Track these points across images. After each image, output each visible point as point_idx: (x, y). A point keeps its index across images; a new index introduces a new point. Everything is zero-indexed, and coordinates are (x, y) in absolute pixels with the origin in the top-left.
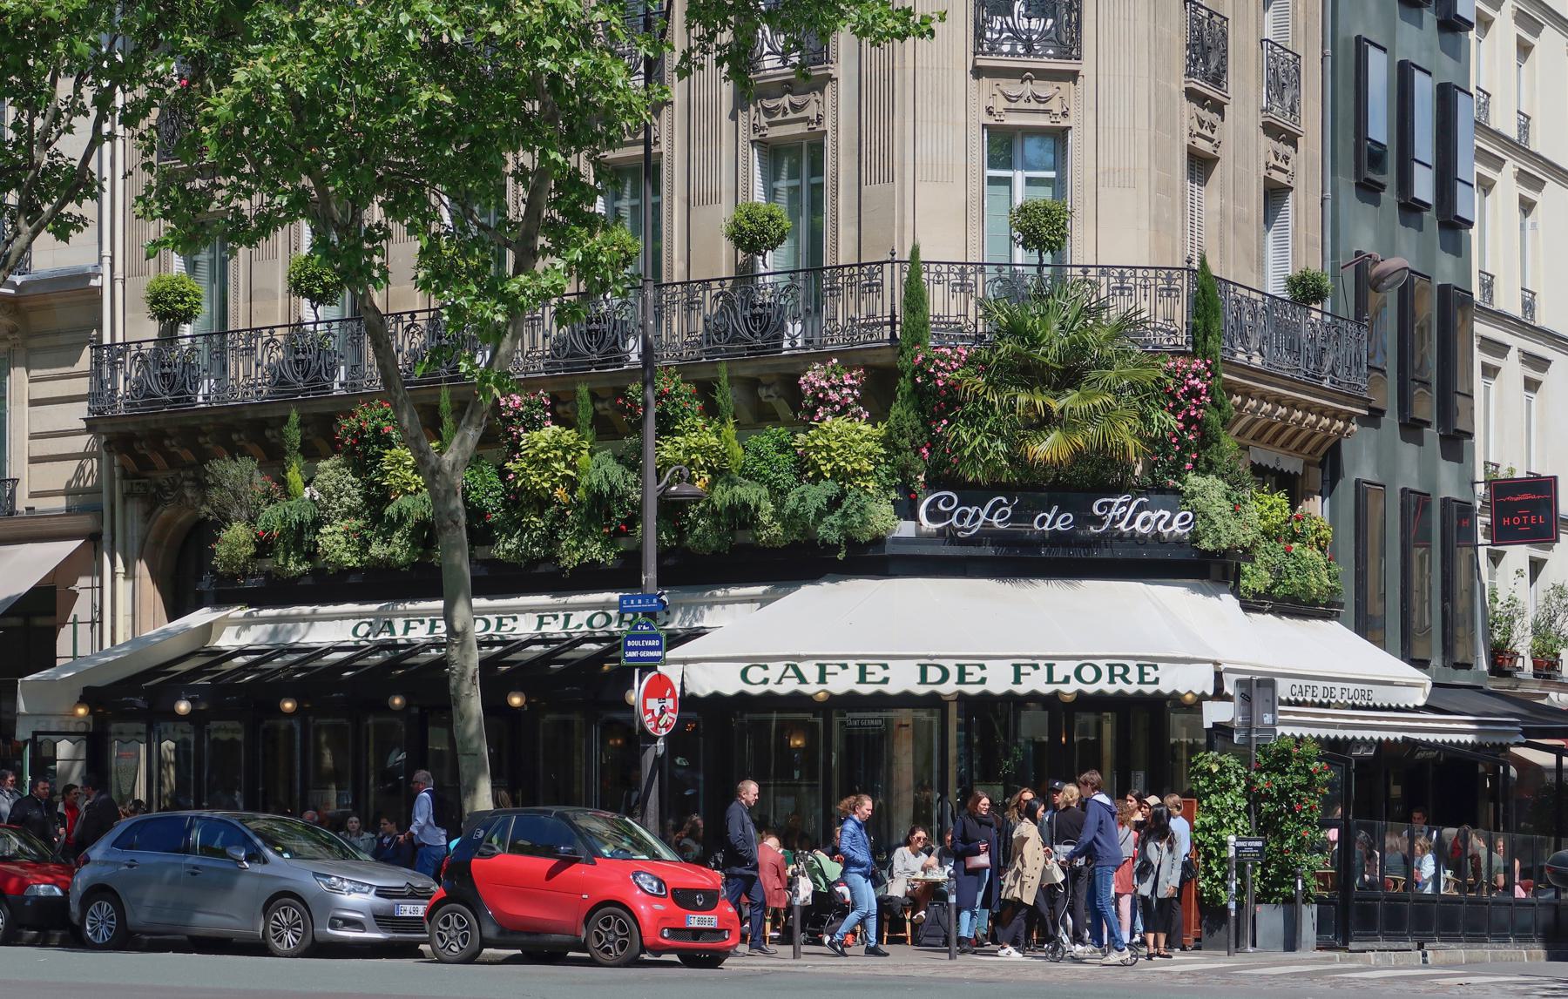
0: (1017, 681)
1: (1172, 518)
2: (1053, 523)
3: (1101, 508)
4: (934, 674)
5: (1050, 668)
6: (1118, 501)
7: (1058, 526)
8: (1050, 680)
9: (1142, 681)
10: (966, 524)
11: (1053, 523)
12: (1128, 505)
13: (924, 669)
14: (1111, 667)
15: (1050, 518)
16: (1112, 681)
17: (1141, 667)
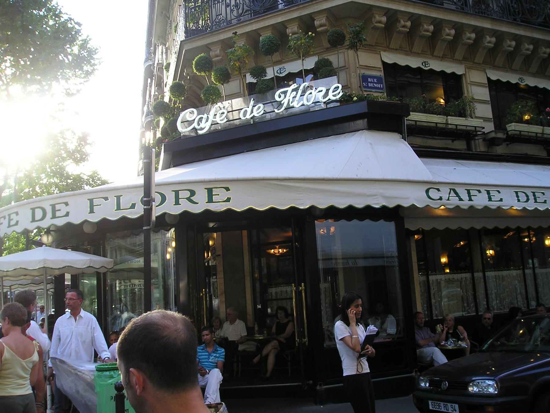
0: (92, 211)
1: (328, 90)
2: (252, 112)
3: (280, 97)
4: (39, 214)
5: (118, 198)
6: (289, 89)
7: (255, 114)
8: (119, 208)
9: (210, 200)
10: (202, 125)
11: (252, 112)
12: (296, 90)
13: (33, 210)
14: (177, 193)
15: (249, 110)
16: (177, 203)
17: (210, 191)
